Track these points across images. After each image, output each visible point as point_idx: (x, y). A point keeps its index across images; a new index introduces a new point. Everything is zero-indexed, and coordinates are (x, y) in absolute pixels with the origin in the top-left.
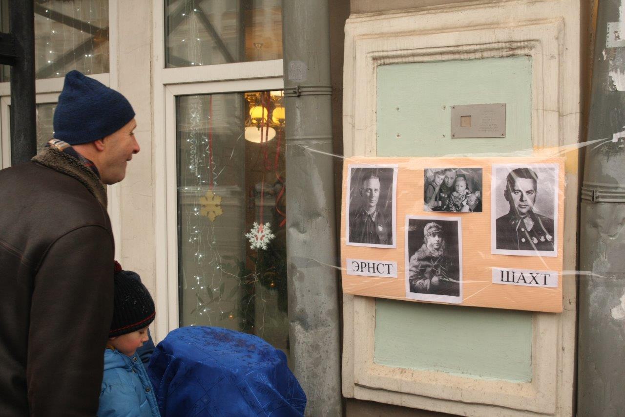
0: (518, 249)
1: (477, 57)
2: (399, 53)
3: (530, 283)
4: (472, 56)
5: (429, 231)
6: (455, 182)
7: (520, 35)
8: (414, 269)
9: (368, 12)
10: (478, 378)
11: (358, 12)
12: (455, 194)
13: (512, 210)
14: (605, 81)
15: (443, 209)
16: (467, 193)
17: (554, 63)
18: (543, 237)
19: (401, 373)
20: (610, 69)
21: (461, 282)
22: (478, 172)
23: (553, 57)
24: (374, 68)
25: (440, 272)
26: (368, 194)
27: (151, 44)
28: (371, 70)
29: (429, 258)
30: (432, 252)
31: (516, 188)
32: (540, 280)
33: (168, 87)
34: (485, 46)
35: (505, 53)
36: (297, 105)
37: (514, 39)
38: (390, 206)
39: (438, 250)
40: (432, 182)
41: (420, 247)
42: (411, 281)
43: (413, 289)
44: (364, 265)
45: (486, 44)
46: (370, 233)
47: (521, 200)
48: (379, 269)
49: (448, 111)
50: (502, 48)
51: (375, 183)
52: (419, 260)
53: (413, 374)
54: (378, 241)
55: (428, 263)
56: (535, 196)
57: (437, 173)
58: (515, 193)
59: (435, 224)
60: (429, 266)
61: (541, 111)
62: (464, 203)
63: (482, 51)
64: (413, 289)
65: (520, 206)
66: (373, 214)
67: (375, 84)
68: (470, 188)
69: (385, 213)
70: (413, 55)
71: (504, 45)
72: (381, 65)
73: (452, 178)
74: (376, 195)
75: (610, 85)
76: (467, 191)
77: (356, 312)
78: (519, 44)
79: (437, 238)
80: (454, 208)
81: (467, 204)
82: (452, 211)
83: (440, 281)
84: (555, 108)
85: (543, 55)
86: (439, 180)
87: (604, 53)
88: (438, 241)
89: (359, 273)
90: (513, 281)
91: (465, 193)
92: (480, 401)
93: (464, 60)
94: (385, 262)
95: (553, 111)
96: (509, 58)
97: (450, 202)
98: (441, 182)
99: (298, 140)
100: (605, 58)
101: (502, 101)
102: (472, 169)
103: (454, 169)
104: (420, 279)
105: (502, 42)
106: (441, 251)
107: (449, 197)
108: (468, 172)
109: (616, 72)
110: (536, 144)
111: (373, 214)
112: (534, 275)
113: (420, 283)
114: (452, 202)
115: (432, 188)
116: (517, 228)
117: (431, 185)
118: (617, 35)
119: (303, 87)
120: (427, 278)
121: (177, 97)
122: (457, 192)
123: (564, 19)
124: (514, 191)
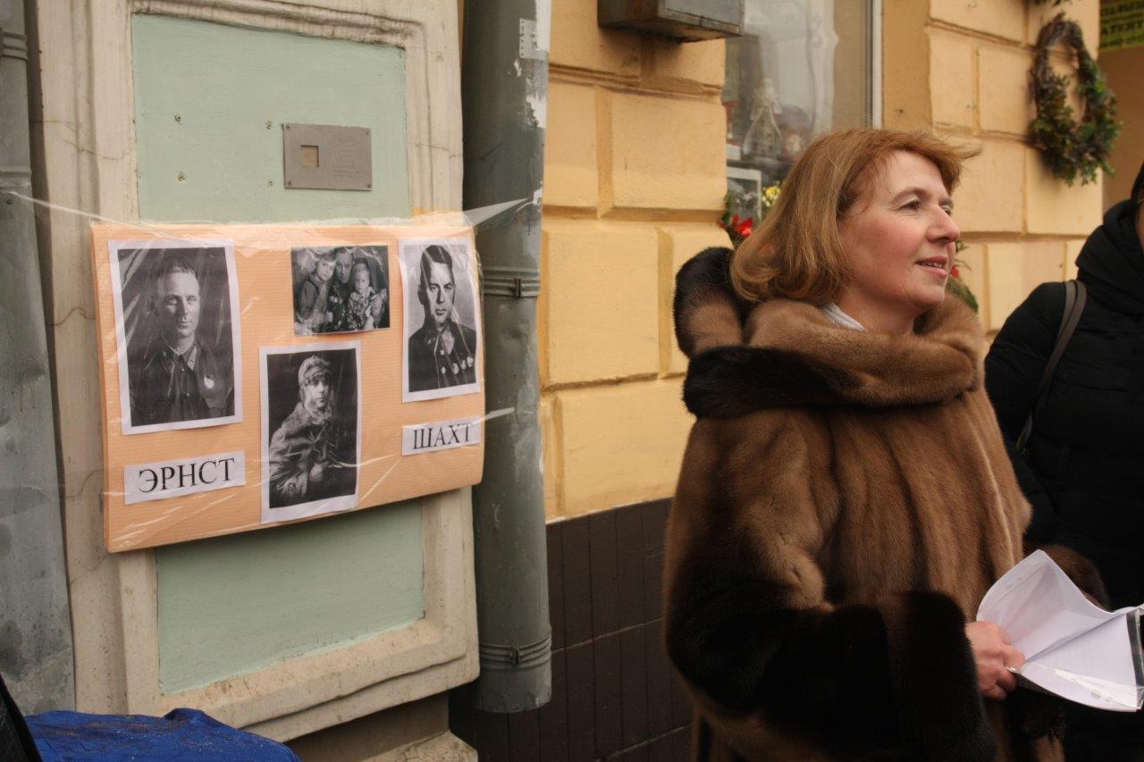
0: (437, 388)
1: (324, 34)
3: (449, 443)
4: (317, 30)
5: (307, 375)
6: (353, 272)
8: (278, 458)
10: (350, 643)
12: (354, 296)
13: (429, 321)
14: (521, 108)
15: (336, 327)
16: (371, 294)
18: (464, 362)
19: (224, 690)
20: (528, 91)
21: (359, 465)
22: (383, 251)
23: (440, 58)
24: (127, 16)
25: (325, 454)
26: (172, 309)
28: (124, 18)
29: (305, 432)
30: (314, 416)
31: (433, 281)
32: (461, 436)
34: (344, 17)
35: (369, 36)
37: (390, 14)
38: (227, 332)
39: (322, 410)
40: (312, 277)
41: (292, 409)
42: (273, 484)
43: (278, 500)
44: (168, 473)
45: (346, 12)
46: (183, 397)
47: (439, 302)
48: (203, 476)
49: (277, 132)
50: (368, 26)
51: (185, 284)
52: (289, 437)
53: (246, 683)
54: (204, 413)
55: (304, 441)
56: (454, 294)
57: (323, 256)
58: (431, 289)
59: (318, 360)
60: (304, 446)
61: (425, 150)
62: (368, 313)
63: (335, 23)
64: (278, 500)
65: (437, 310)
66: (190, 352)
67: (130, 56)
68: (375, 284)
69: (217, 347)
71: (371, 21)
72: (138, 13)
73: (347, 266)
74: (192, 310)
75: (528, 116)
76: (370, 289)
77: (127, 590)
78: (393, 25)
79: (321, 387)
80: (354, 324)
81: (371, 314)
82: (353, 329)
83: (326, 472)
85: (425, 48)
86: (326, 271)
87: (516, 65)
88: (323, 393)
89: (158, 493)
90: (429, 446)
91: (368, 294)
92: (369, 682)
93: (298, 34)
94: (217, 457)
96: (370, 46)
97: (347, 312)
98: (331, 273)
100: (519, 74)
101: (365, 125)
102: (377, 248)
103: (350, 248)
104: (290, 476)
105: (370, 15)
106: (329, 411)
107: (346, 302)
108: (371, 253)
110: (417, 204)
111: (190, 352)
112: (454, 428)
113: (290, 484)
114: (351, 312)
115: (313, 289)
116: (435, 350)
117: (309, 280)
120: (302, 472)
122: (358, 293)
124: (430, 284)
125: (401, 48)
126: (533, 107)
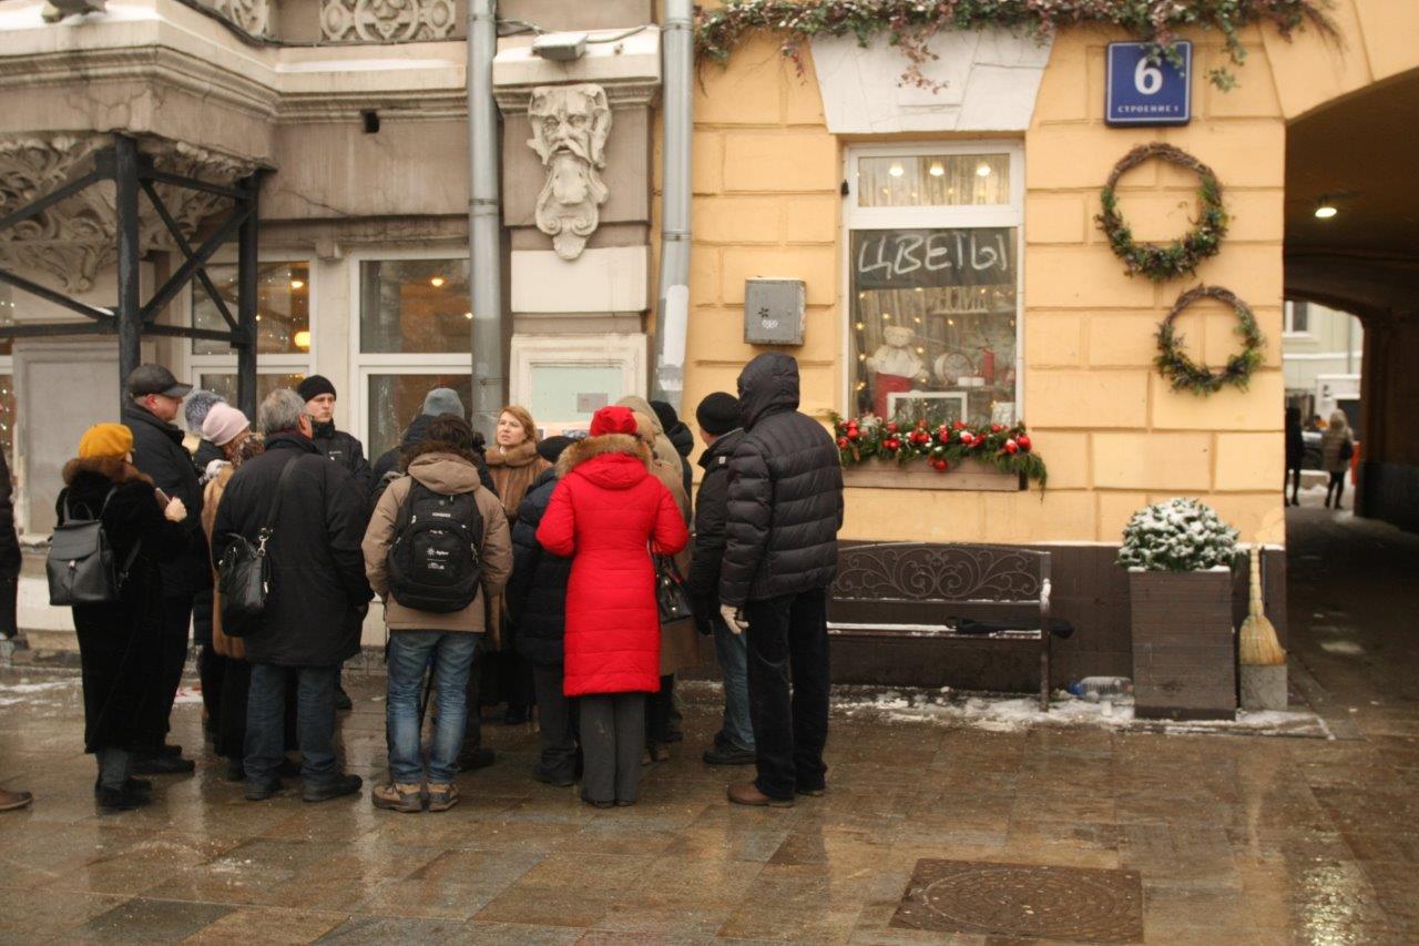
7: (615, 356)
11: (520, 333)
27: (348, 334)
121: (370, 376)
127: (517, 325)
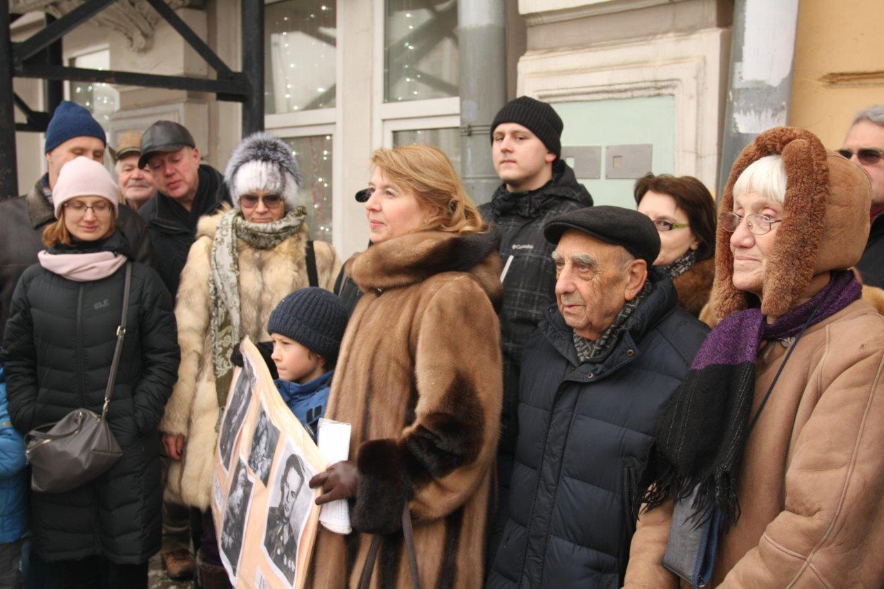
2: (561, 92)
4: (624, 95)
7: (663, 74)
9: (542, 49)
11: (534, 49)
17: (693, 103)
23: (691, 97)
27: (371, 79)
33: (386, 122)
35: (652, 92)
36: (468, 144)
37: (658, 78)
70: (573, 94)
78: (663, 84)
84: (692, 148)
87: (731, 94)
95: (691, 152)
99: (469, 178)
100: (731, 99)
101: (649, 142)
109: (739, 113)
118: (740, 75)
119: (473, 126)
121: (395, 132)
123: (705, 57)
125: (672, 95)
126: (737, 121)
127: (534, 37)
